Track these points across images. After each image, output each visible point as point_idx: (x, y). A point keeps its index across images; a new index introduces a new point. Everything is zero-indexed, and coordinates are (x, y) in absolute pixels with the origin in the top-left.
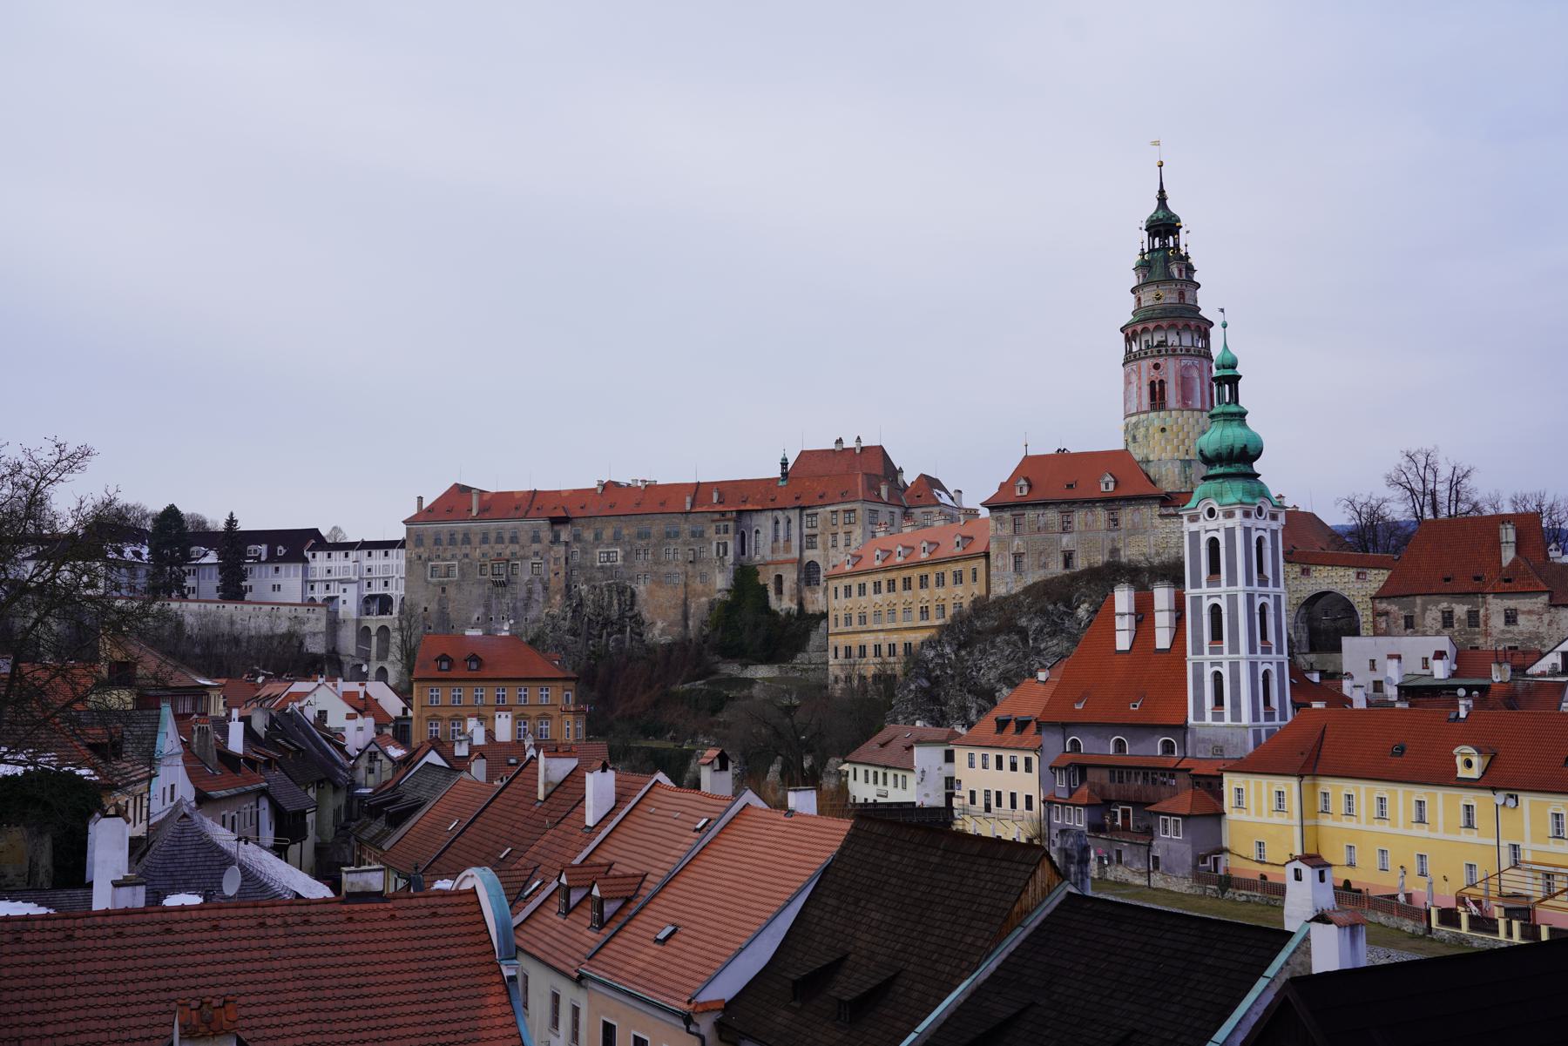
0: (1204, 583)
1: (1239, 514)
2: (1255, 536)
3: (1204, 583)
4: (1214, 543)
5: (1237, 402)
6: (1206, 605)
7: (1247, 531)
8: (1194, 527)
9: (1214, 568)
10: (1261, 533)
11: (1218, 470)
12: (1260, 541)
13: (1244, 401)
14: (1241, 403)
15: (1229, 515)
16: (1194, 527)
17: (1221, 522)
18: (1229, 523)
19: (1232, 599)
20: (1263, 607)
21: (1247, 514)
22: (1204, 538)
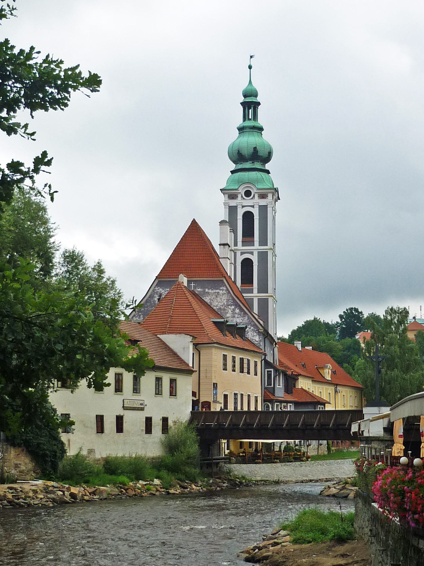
8: (233, 203)
9: (248, 233)
11: (248, 165)
13: (261, 121)
14: (259, 122)
15: (263, 196)
16: (233, 203)
17: (258, 201)
18: (263, 202)
22: (240, 212)
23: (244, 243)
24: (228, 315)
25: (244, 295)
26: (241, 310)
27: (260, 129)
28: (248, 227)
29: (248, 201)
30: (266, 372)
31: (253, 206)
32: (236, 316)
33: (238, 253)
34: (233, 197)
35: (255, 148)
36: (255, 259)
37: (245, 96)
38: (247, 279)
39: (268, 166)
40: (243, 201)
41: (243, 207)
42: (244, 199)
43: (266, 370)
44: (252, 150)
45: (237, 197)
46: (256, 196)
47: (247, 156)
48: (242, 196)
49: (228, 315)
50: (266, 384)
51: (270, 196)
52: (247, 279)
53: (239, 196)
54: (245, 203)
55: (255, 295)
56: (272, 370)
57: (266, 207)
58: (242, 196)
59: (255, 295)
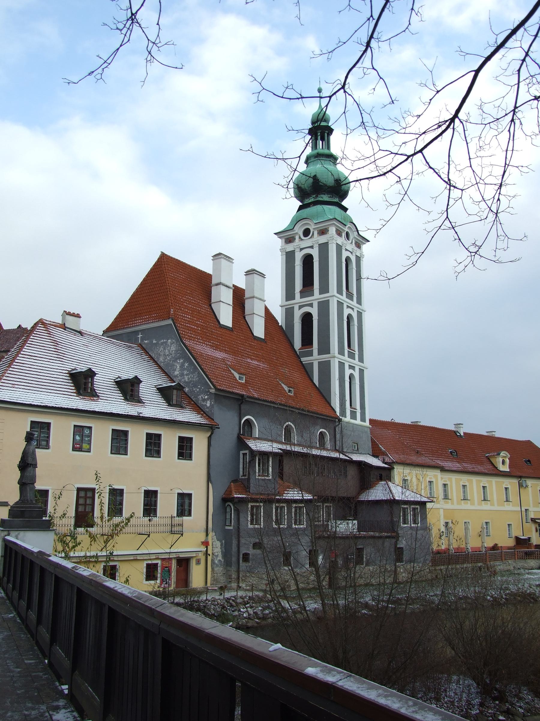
0: (298, 295)
1: (332, 230)
2: (345, 254)
3: (298, 295)
4: (308, 260)
5: (329, 147)
6: (298, 314)
7: (339, 248)
10: (348, 254)
12: (348, 260)
15: (323, 232)
16: (290, 247)
18: (323, 239)
19: (324, 306)
20: (349, 317)
21: (339, 233)
23: (303, 294)
24: (177, 373)
25: (303, 359)
26: (191, 363)
27: (333, 158)
28: (305, 273)
29: (307, 242)
30: (241, 456)
31: (312, 247)
32: (185, 372)
33: (296, 307)
34: (289, 240)
35: (315, 178)
36: (314, 311)
37: (312, 124)
38: (307, 340)
39: (344, 203)
40: (301, 243)
41: (301, 249)
42: (302, 240)
43: (241, 452)
44: (311, 180)
45: (295, 239)
46: (316, 233)
47: (307, 188)
48: (300, 238)
49: (177, 373)
50: (241, 473)
51: (332, 230)
52: (307, 340)
53: (297, 238)
54: (304, 244)
55: (315, 358)
56: (247, 452)
57: (326, 244)
58: (300, 238)
59: (315, 358)
